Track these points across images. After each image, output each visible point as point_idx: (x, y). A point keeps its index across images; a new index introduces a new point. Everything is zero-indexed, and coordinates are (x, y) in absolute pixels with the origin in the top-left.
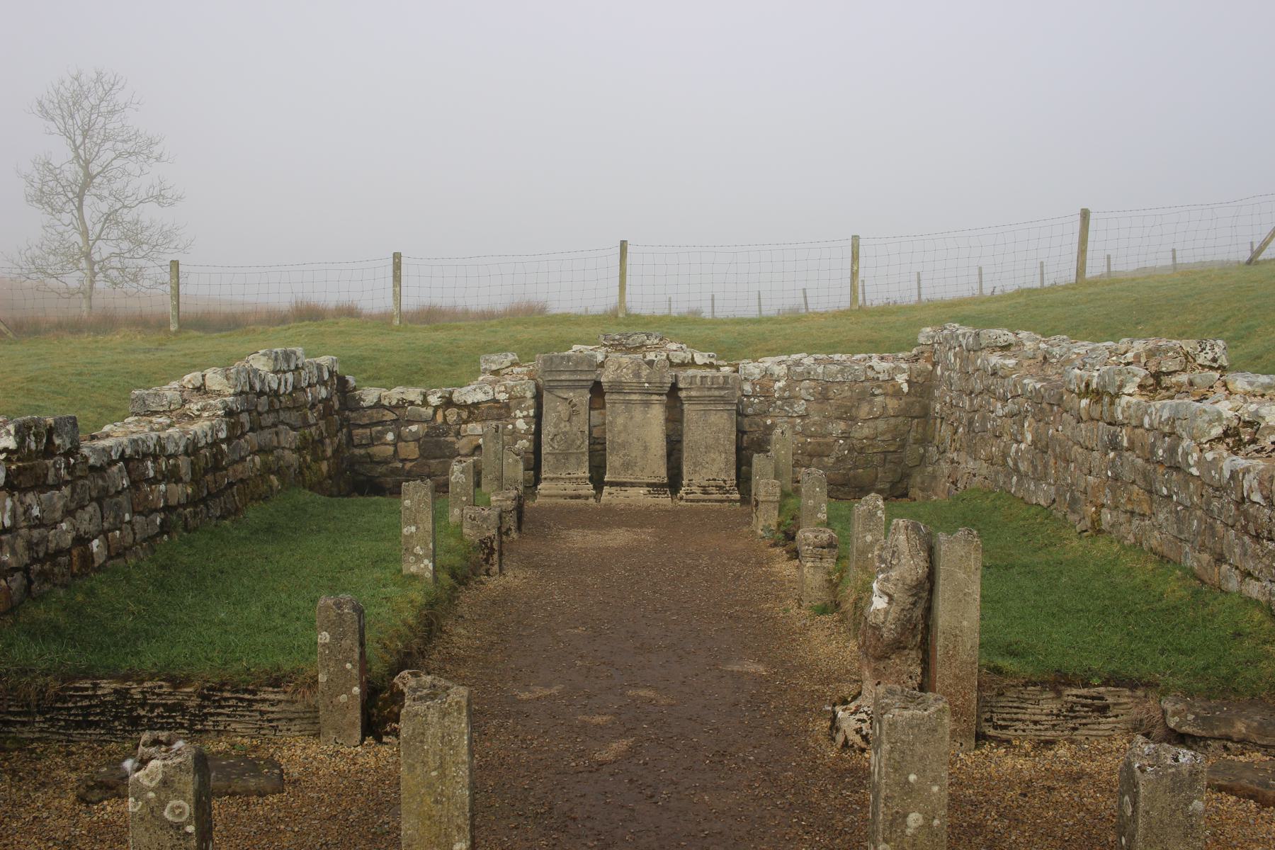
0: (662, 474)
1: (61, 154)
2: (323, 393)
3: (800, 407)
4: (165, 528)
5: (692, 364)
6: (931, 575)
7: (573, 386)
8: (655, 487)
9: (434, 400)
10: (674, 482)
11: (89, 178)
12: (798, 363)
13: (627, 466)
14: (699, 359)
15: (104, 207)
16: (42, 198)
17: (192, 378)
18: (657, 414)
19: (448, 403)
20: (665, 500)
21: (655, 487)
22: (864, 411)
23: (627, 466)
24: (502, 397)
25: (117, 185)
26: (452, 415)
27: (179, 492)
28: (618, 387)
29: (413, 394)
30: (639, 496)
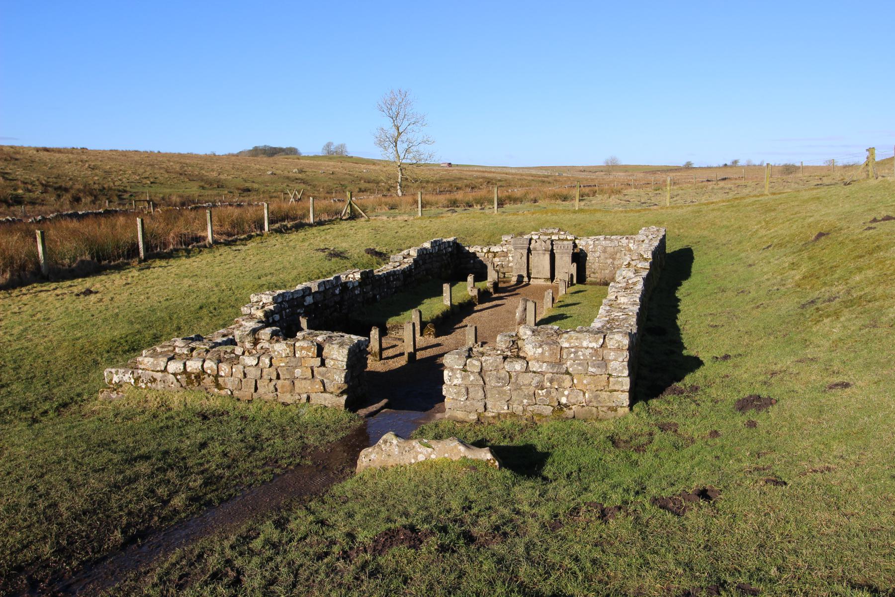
0: (549, 276)
1: (388, 124)
2: (450, 249)
3: (597, 254)
4: (395, 292)
5: (567, 240)
6: (525, 309)
7: (522, 248)
8: (547, 279)
9: (485, 250)
10: (552, 277)
11: (399, 134)
12: (598, 240)
13: (538, 273)
14: (569, 238)
15: (405, 146)
16: (381, 143)
17: (405, 252)
18: (547, 257)
19: (489, 252)
20: (549, 283)
21: (547, 279)
22: (618, 254)
23: (538, 273)
24: (505, 250)
25: (410, 136)
26: (491, 255)
27: (398, 283)
28: (535, 249)
29: (479, 249)
30: (541, 282)
